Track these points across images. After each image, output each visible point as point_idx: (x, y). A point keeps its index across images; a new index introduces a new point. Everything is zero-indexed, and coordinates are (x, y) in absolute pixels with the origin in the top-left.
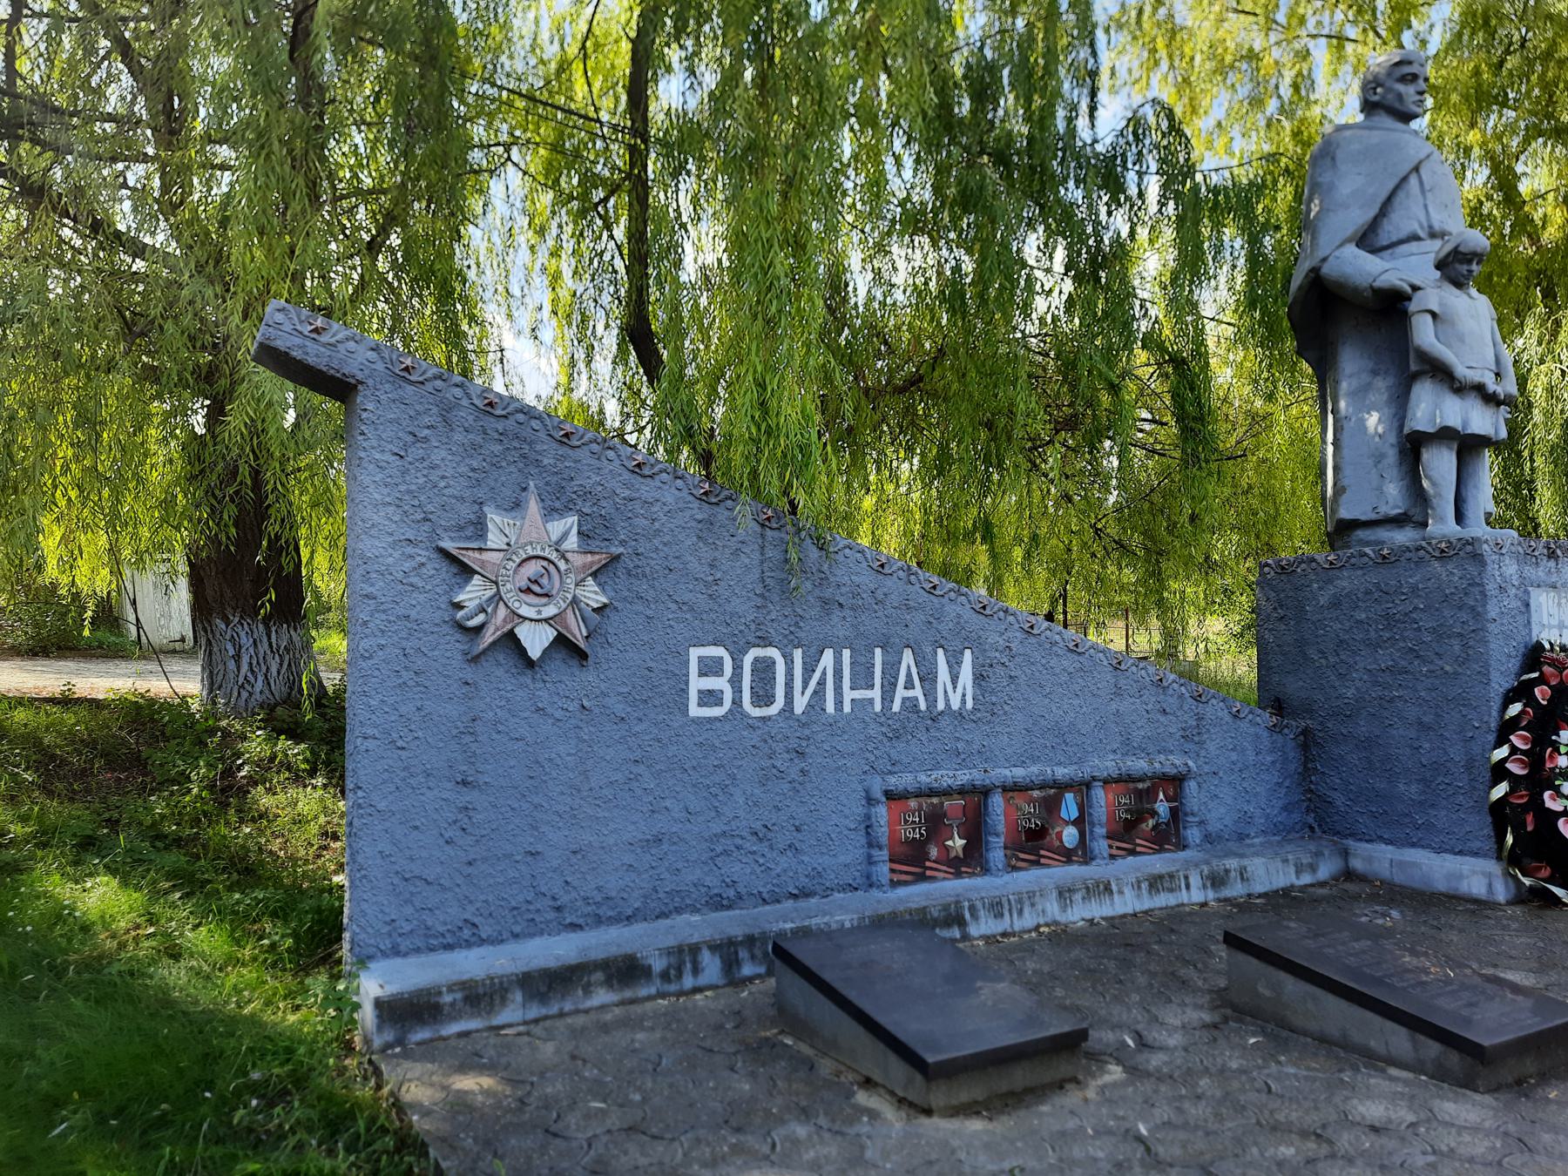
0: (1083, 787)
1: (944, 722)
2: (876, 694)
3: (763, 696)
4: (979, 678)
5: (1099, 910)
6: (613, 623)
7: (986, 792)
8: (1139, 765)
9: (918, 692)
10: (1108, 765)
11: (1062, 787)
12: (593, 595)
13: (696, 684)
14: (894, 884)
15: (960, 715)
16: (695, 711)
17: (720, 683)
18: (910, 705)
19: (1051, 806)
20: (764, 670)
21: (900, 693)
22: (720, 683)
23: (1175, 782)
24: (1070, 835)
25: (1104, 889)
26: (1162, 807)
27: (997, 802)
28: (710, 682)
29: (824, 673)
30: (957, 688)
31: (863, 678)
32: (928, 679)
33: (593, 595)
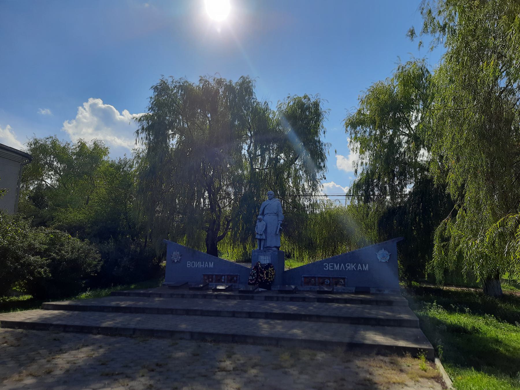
0: (224, 276)
3: (193, 266)
7: (212, 275)
8: (232, 274)
10: (228, 274)
11: (222, 276)
12: (180, 258)
19: (221, 278)
20: (193, 263)
23: (237, 276)
24: (223, 280)
26: (235, 278)
27: (214, 276)
28: (189, 264)
30: (211, 265)
31: (202, 264)
32: (209, 264)
33: (180, 258)
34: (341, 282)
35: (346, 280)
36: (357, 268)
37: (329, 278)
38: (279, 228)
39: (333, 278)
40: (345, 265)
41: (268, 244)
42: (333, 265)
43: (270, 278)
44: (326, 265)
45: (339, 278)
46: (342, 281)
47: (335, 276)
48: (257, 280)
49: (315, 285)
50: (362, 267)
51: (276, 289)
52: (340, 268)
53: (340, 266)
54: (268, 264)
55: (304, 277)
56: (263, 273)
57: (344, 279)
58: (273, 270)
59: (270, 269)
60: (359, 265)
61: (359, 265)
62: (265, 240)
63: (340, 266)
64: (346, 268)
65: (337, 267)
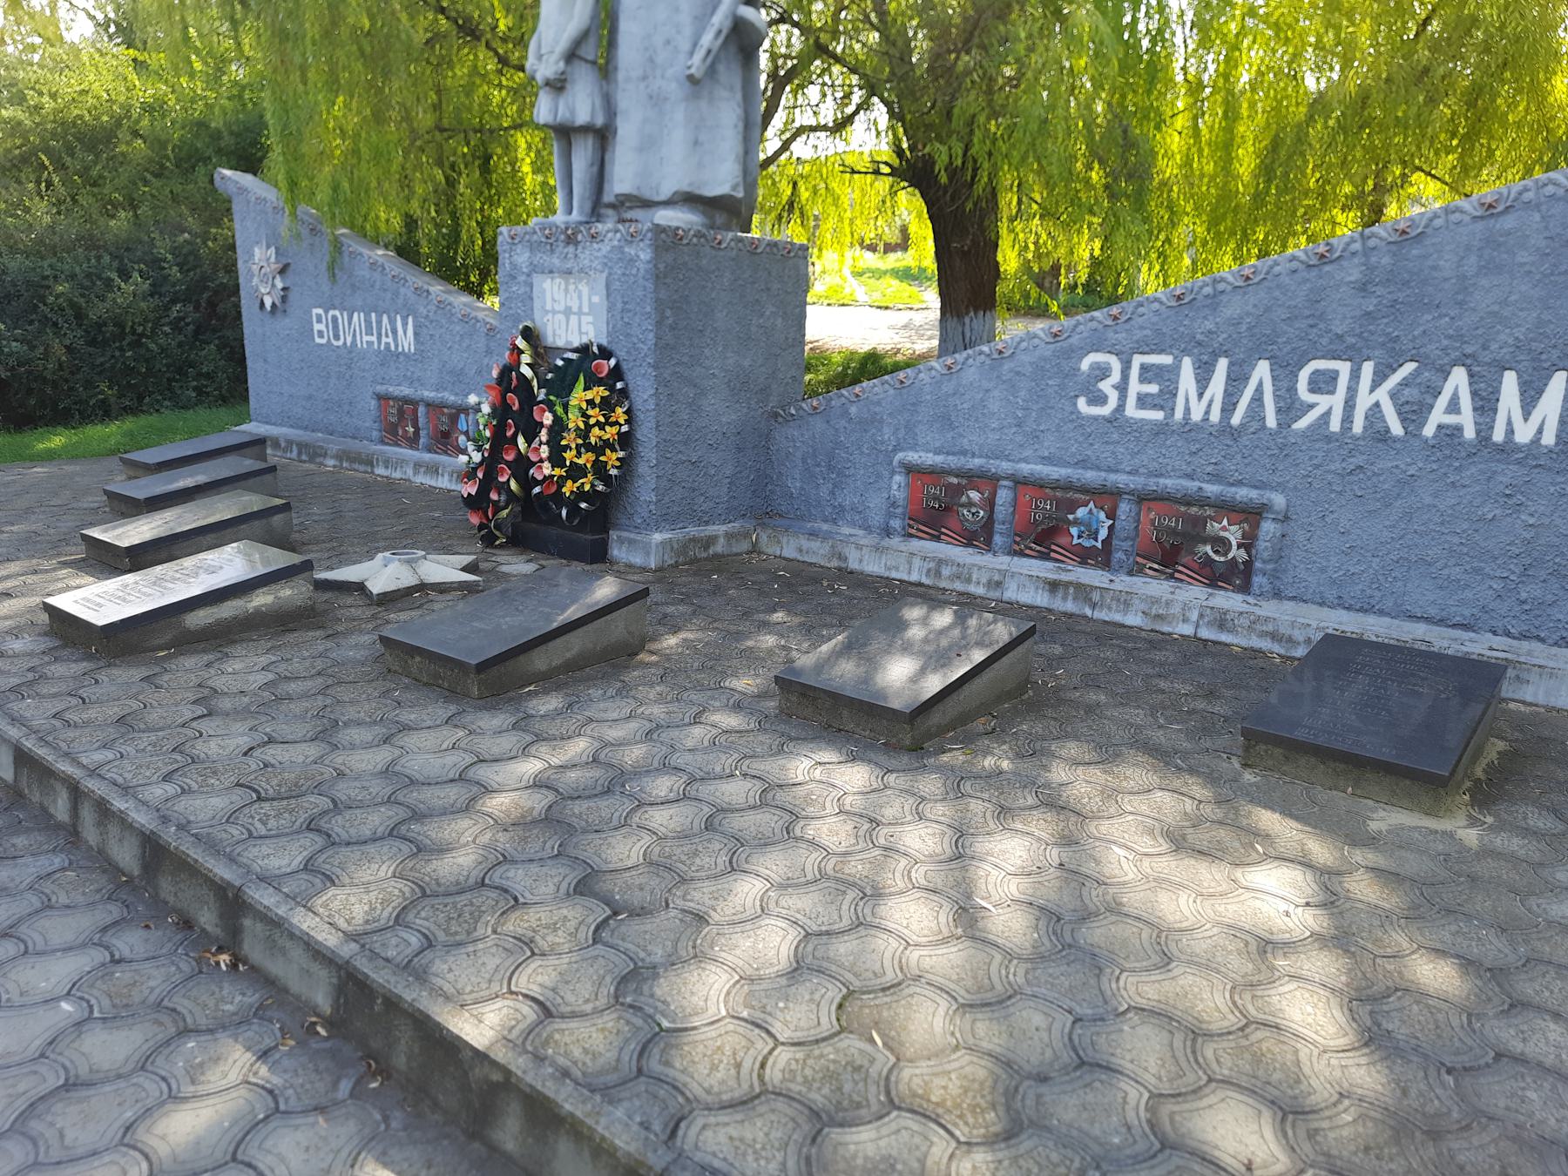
1: (402, 358)
2: (374, 339)
3: (337, 337)
4: (416, 334)
5: (429, 481)
6: (292, 296)
7: (414, 403)
9: (390, 340)
12: (279, 284)
13: (317, 327)
14: (382, 442)
15: (407, 356)
16: (318, 340)
17: (322, 327)
18: (387, 344)
20: (335, 319)
21: (384, 340)
22: (322, 327)
25: (434, 470)
27: (421, 410)
29: (1260, 384)
34: (1221, 544)
35: (1268, 528)
36: (1413, 413)
37: (1108, 497)
38: (720, 19)
39: (1143, 498)
40: (1285, 371)
41: (622, 180)
42: (1166, 377)
43: (576, 472)
44: (1102, 372)
45: (1203, 502)
46: (1233, 535)
47: (1170, 483)
48: (488, 483)
49: (988, 546)
50: (1486, 404)
51: (637, 560)
52: (1229, 407)
53: (1236, 380)
54: (584, 350)
55: (910, 470)
56: (531, 432)
57: (1251, 515)
58: (606, 405)
59: (579, 396)
60: (1459, 378)
61: (1459, 378)
62: (603, 136)
63: (1236, 380)
64: (1290, 407)
65: (1199, 399)
